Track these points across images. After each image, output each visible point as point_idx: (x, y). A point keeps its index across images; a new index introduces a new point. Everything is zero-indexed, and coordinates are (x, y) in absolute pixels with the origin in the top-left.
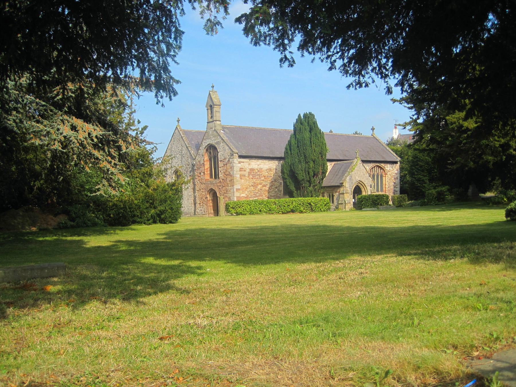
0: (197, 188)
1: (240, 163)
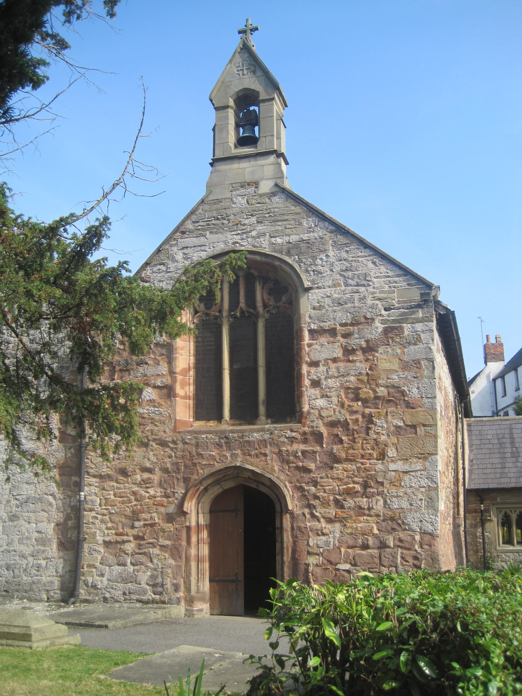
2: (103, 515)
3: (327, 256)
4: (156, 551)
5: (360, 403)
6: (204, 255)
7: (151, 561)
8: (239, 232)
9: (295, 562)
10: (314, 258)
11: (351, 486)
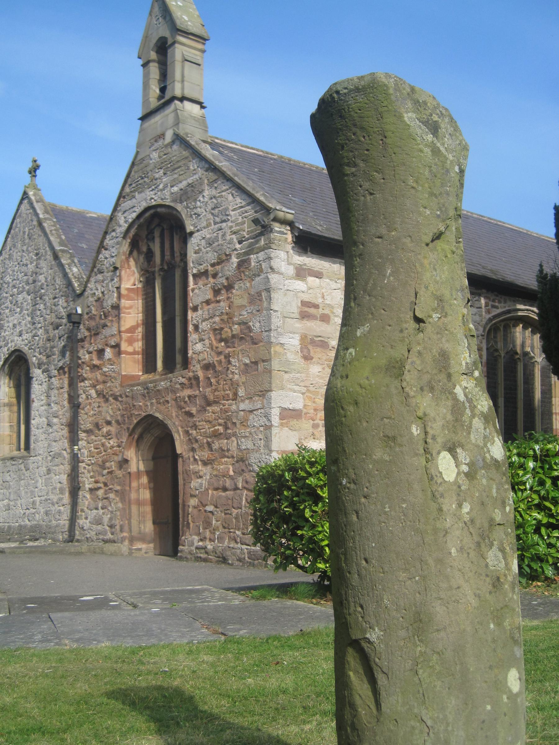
1: (301, 273)
3: (203, 196)
4: (112, 496)
5: (223, 344)
6: (134, 215)
8: (153, 187)
10: (195, 201)
11: (216, 428)
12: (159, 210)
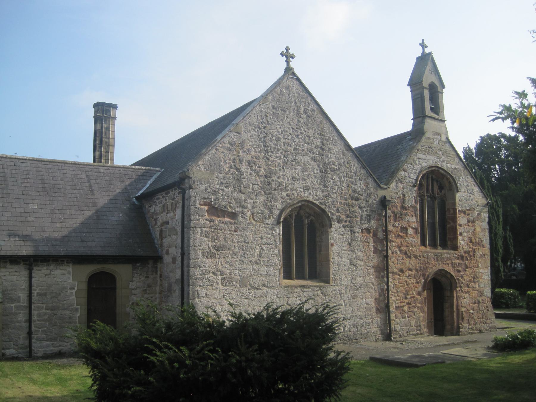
0: (393, 266)
2: (395, 293)
7: (414, 315)
9: (458, 310)
12: (440, 170)
